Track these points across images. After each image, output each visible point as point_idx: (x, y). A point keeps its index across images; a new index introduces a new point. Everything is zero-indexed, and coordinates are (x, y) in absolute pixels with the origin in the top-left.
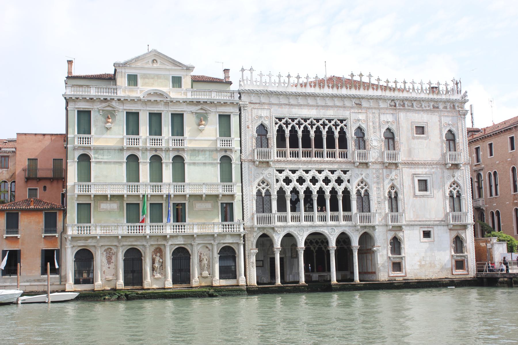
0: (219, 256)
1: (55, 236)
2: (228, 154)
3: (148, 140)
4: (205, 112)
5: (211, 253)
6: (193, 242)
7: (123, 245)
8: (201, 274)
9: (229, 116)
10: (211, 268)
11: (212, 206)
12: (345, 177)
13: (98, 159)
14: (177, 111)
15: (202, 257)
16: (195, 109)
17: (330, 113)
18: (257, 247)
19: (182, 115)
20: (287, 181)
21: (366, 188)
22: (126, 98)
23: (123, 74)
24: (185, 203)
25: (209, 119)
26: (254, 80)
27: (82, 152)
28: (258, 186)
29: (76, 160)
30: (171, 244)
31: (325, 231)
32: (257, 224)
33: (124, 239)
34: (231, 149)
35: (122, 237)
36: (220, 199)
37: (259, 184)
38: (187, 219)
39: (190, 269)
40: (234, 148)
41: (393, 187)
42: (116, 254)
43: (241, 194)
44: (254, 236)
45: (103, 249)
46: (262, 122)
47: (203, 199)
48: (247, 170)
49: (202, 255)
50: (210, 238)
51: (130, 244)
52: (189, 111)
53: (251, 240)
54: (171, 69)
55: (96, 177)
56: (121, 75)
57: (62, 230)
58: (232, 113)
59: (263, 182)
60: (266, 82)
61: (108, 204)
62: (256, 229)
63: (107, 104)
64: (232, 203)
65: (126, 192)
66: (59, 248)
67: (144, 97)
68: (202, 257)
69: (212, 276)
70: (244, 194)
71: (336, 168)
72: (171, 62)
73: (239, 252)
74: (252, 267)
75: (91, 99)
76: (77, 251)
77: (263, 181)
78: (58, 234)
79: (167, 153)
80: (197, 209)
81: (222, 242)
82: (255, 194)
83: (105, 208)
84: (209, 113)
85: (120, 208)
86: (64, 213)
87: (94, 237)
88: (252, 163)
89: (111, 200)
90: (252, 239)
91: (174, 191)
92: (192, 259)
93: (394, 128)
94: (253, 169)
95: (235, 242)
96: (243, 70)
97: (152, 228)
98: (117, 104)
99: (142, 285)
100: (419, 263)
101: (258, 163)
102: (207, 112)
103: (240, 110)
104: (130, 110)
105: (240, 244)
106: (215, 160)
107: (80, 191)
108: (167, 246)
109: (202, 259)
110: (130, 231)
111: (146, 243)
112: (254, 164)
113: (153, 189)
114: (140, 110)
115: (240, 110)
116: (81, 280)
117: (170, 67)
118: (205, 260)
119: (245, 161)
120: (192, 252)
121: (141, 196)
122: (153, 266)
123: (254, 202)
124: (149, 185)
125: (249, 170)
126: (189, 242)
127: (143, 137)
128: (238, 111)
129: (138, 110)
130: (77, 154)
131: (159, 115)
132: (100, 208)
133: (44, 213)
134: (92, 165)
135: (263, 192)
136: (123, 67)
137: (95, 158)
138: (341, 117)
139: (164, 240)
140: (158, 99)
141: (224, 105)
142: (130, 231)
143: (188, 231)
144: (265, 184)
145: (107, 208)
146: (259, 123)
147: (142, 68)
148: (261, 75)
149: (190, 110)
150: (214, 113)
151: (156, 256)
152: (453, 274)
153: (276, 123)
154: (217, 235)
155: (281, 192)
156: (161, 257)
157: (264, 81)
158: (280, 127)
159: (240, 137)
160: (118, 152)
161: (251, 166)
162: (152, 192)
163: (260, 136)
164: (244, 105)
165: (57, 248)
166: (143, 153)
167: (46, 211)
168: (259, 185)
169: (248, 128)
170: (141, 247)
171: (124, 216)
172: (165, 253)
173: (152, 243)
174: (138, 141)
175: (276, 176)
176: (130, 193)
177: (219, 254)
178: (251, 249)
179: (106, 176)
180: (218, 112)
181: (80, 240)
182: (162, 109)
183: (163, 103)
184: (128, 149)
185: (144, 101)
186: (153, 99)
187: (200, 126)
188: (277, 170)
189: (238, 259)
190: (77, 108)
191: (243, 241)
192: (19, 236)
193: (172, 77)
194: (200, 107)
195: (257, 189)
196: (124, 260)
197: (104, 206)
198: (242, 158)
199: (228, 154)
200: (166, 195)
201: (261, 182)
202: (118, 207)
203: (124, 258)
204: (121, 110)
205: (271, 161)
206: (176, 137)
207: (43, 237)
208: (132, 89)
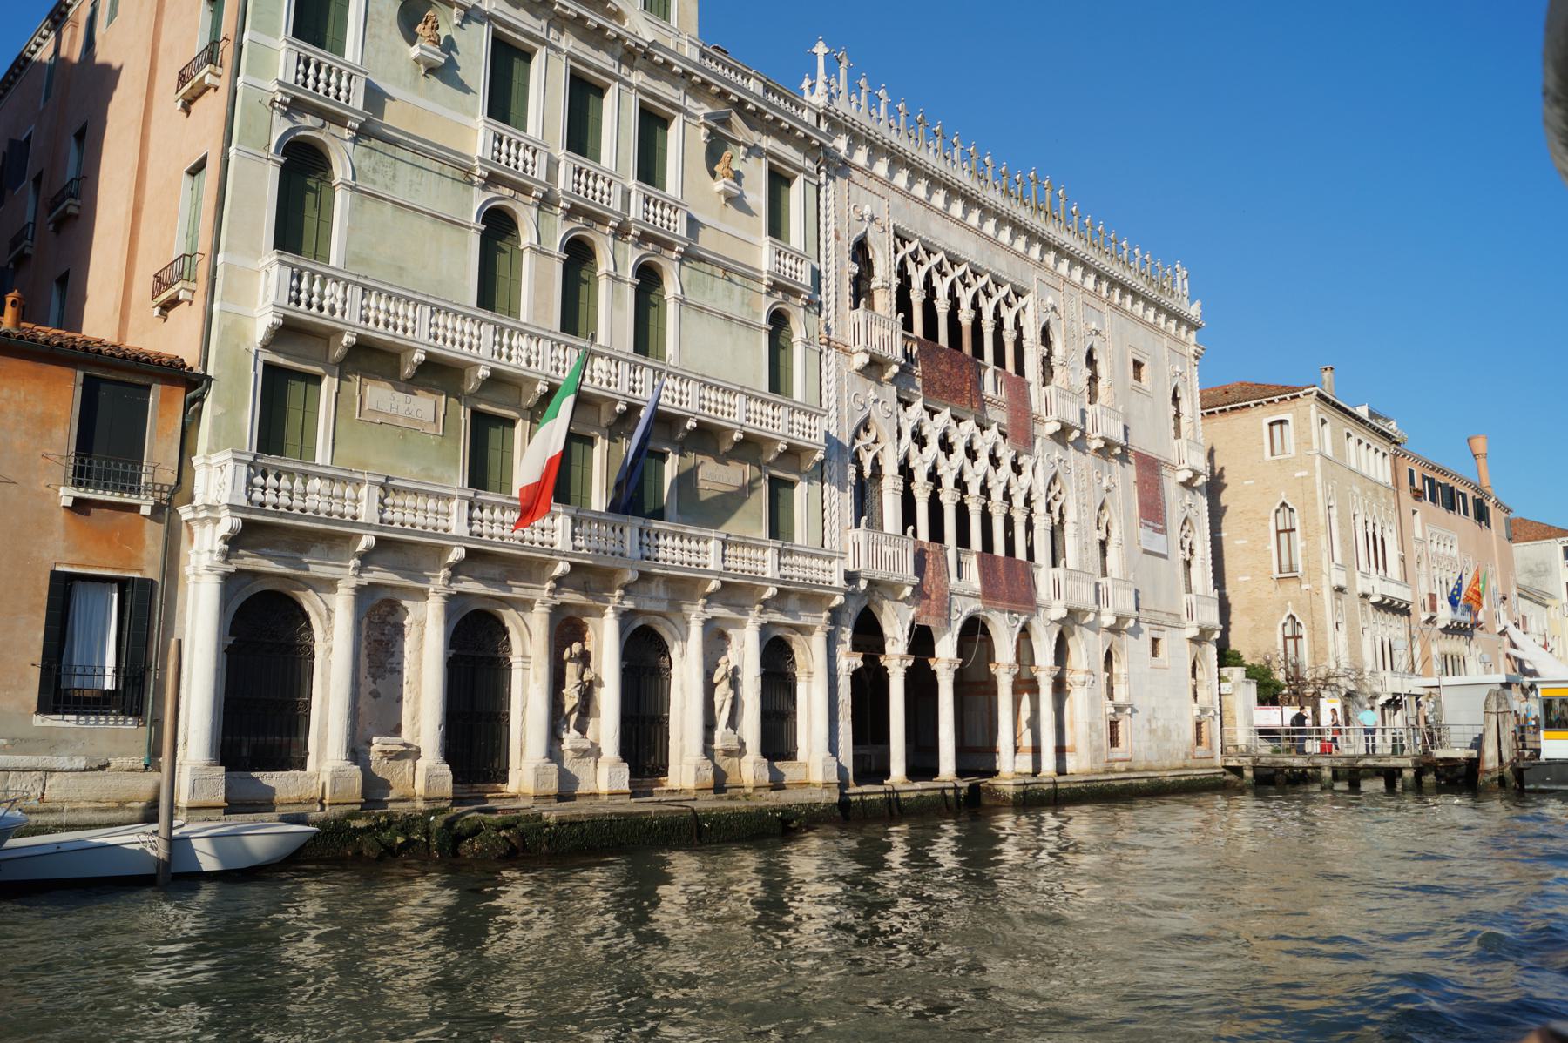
13: (374, 183)
55: (351, 258)
58: (801, 170)
65: (489, 356)
66: (152, 572)
86: (191, 395)
133: (80, 374)
144: (872, 436)
145: (394, 412)
158: (903, 262)
165: (137, 575)
179: (401, 268)
205: (897, 363)
207: (69, 502)
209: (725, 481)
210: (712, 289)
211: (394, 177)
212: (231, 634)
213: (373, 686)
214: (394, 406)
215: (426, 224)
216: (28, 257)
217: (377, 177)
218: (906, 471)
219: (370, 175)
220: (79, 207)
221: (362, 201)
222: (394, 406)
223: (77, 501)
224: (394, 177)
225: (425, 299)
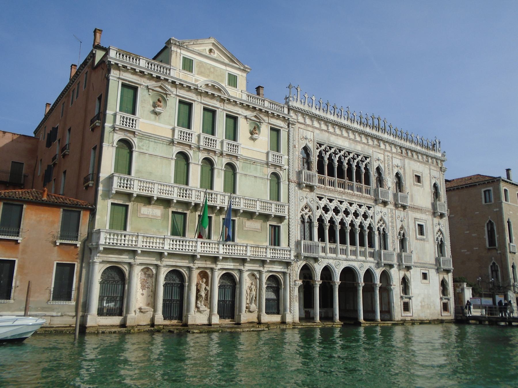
1: (76, 244)
4: (259, 121)
12: (370, 213)
13: (143, 149)
16: (248, 113)
17: (359, 148)
18: (300, 279)
20: (326, 209)
21: (384, 225)
22: (182, 83)
23: (178, 54)
31: (355, 265)
34: (281, 167)
38: (237, 240)
40: (284, 165)
41: (402, 228)
51: (174, 264)
52: (243, 116)
53: (296, 270)
55: (138, 172)
56: (176, 55)
59: (306, 208)
61: (150, 210)
67: (201, 86)
71: (363, 203)
72: (228, 57)
83: (146, 213)
87: (133, 253)
93: (401, 172)
97: (203, 245)
100: (420, 304)
107: (120, 186)
108: (215, 269)
128: (287, 127)
130: (118, 136)
131: (213, 112)
133: (62, 210)
135: (306, 217)
136: (179, 47)
137: (139, 147)
138: (366, 154)
140: (216, 94)
143: (238, 252)
145: (148, 214)
152: (441, 316)
153: (317, 149)
155: (321, 220)
158: (320, 152)
167: (66, 208)
168: (302, 210)
169: (295, 147)
174: (190, 136)
175: (317, 202)
186: (210, 92)
188: (318, 197)
192: (20, 239)
195: (301, 214)
197: (146, 210)
202: (162, 215)
207: (58, 244)
208: (187, 75)
209: (254, 227)
210: (250, 168)
211: (149, 146)
213: (142, 292)
216: (56, 164)
217: (144, 148)
218: (321, 220)
220: (69, 152)
223: (61, 244)
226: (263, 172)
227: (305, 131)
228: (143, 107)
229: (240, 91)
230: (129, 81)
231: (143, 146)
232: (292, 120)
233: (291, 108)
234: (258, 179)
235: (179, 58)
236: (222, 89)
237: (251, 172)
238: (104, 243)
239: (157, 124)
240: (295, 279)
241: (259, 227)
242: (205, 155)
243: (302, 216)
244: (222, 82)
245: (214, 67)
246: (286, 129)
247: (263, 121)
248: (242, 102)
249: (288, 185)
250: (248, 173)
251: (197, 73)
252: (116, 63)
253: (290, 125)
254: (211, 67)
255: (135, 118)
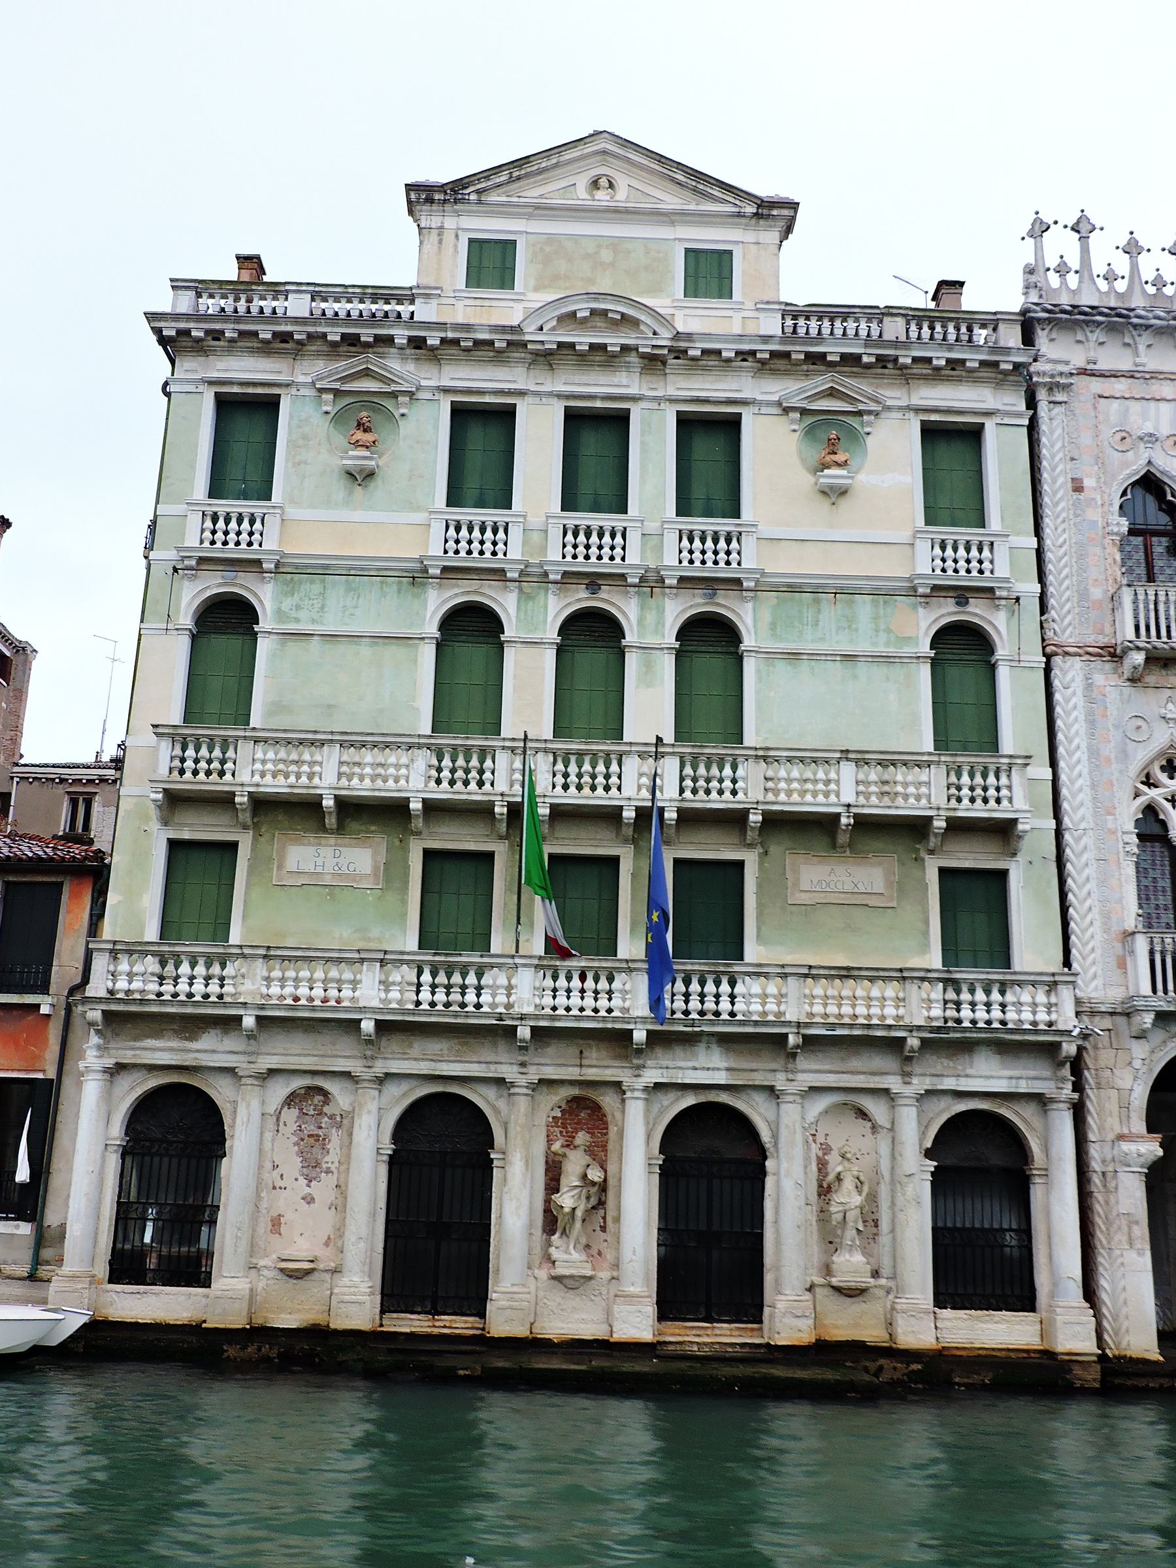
0: (931, 1165)
1: (37, 1007)
2: (976, 615)
3: (555, 534)
5: (884, 1149)
6: (781, 1076)
7: (387, 1075)
8: (827, 1270)
9: (972, 435)
10: (885, 1239)
11: (889, 884)
13: (297, 620)
14: (706, 401)
15: (830, 1167)
18: (1152, 1127)
19: (730, 427)
23: (449, 237)
24: (740, 865)
25: (869, 440)
26: (1099, 268)
27: (213, 584)
28: (1144, 788)
29: (186, 619)
30: (658, 1086)
32: (1154, 990)
33: (392, 1044)
34: (991, 590)
35: (381, 1026)
36: (933, 842)
37: (1148, 776)
38: (753, 951)
39: (760, 1237)
40: (1007, 580)
42: (344, 1122)
43: (1052, 824)
44: (1137, 1064)
45: (280, 1090)
46: (1149, 462)
47: (842, 839)
48: (1078, 700)
49: (833, 1159)
50: (879, 1061)
51: (424, 1068)
52: (769, 404)
53: (1120, 1084)
54: (682, 213)
55: (276, 708)
56: (440, 242)
57: (78, 980)
58: (988, 414)
60: (1159, 277)
62: (1149, 1019)
63: (354, 364)
64: (1001, 876)
66: (51, 1074)
67: (541, 329)
68: (835, 1166)
69: (891, 1284)
70: (1067, 821)
73: (1046, 1149)
74: (1131, 1243)
75: (285, 337)
76: (139, 1091)
77: (1170, 761)
78: (49, 999)
79: (652, 602)
80: (803, 895)
81: (949, 1083)
82: (1130, 826)
84: (870, 412)
85: (386, 870)
88: (1108, 666)
89: (340, 829)
90: (1124, 1079)
91: (682, 791)
92: (777, 1174)
94: (1112, 695)
95: (1023, 1087)
96: (1039, 229)
98: (411, 367)
99: (482, 1315)
101: (1139, 658)
102: (861, 407)
103: (1032, 403)
104: (469, 391)
105: (1052, 1100)
106: (908, 640)
109: (831, 1177)
110: (425, 995)
111: (516, 1068)
112: (1115, 671)
113: (566, 775)
114: (522, 393)
115: (1032, 403)
116: (152, 1262)
117: (672, 200)
118: (848, 1184)
119: (1067, 654)
120: (775, 1136)
121: (500, 810)
122: (548, 1201)
123: (1130, 870)
124: (546, 751)
125: (1090, 700)
126: (759, 1079)
127: (536, 520)
128: (1022, 406)
129: (510, 393)
132: (280, 867)
134: (264, 647)
136: (448, 207)
139: (618, 1057)
140: (613, 340)
141: (948, 379)
142: (425, 995)
145: (319, 870)
146: (1135, 468)
147: (541, 210)
148: (1132, 249)
149: (775, 398)
150: (894, 415)
151: (569, 1145)
154: (923, 1040)
156: (599, 1152)
157: (1148, 274)
159: (1038, 531)
160: (399, 591)
161: (1099, 679)
162: (559, 789)
163: (1141, 539)
164: (1052, 376)
165: (40, 1076)
166: (524, 596)
169: (1078, 488)
170: (491, 1092)
171: (404, 915)
172: (621, 1134)
173: (551, 1073)
176: (443, 793)
177: (929, 1154)
178: (1121, 1137)
179: (329, 706)
180: (918, 410)
181: (157, 1035)
182: (633, 390)
183: (633, 358)
184: (450, 572)
185: (539, 347)
186: (583, 339)
187: (826, 472)
189: (1048, 1193)
190: (211, 383)
191: (1070, 1086)
193: (688, 251)
194: (822, 381)
195: (1142, 800)
196: (395, 1163)
198: (1049, 634)
199: (977, 612)
200: (638, 809)
201: (1163, 768)
202: (376, 868)
203: (388, 1148)
204: (429, 396)
206: (700, 520)
208: (487, 303)
209: (849, 887)
211: (322, 608)
212: (126, 1134)
214: (320, 862)
215: (365, 650)
217: (303, 615)
219: (293, 614)
221: (283, 644)
222: (320, 862)
224: (322, 608)
225: (330, 737)
226: (888, 631)
227: (1135, 406)
228: (299, 464)
229: (750, 305)
230: (243, 384)
231: (298, 607)
232: (1047, 367)
233: (1039, 320)
234: (862, 668)
235: (451, 250)
236: (642, 318)
237: (822, 639)
238: (103, 993)
239: (359, 515)
240: (1114, 1125)
241: (879, 886)
242: (579, 599)
243: (1150, 810)
244: (656, 289)
245: (615, 244)
246: (1019, 415)
247: (873, 407)
248: (746, 347)
249: (1048, 670)
250: (810, 647)
251: (532, 282)
252: (180, 332)
253: (1042, 395)
254: (599, 246)
255: (258, 512)
